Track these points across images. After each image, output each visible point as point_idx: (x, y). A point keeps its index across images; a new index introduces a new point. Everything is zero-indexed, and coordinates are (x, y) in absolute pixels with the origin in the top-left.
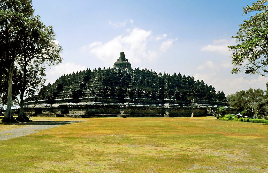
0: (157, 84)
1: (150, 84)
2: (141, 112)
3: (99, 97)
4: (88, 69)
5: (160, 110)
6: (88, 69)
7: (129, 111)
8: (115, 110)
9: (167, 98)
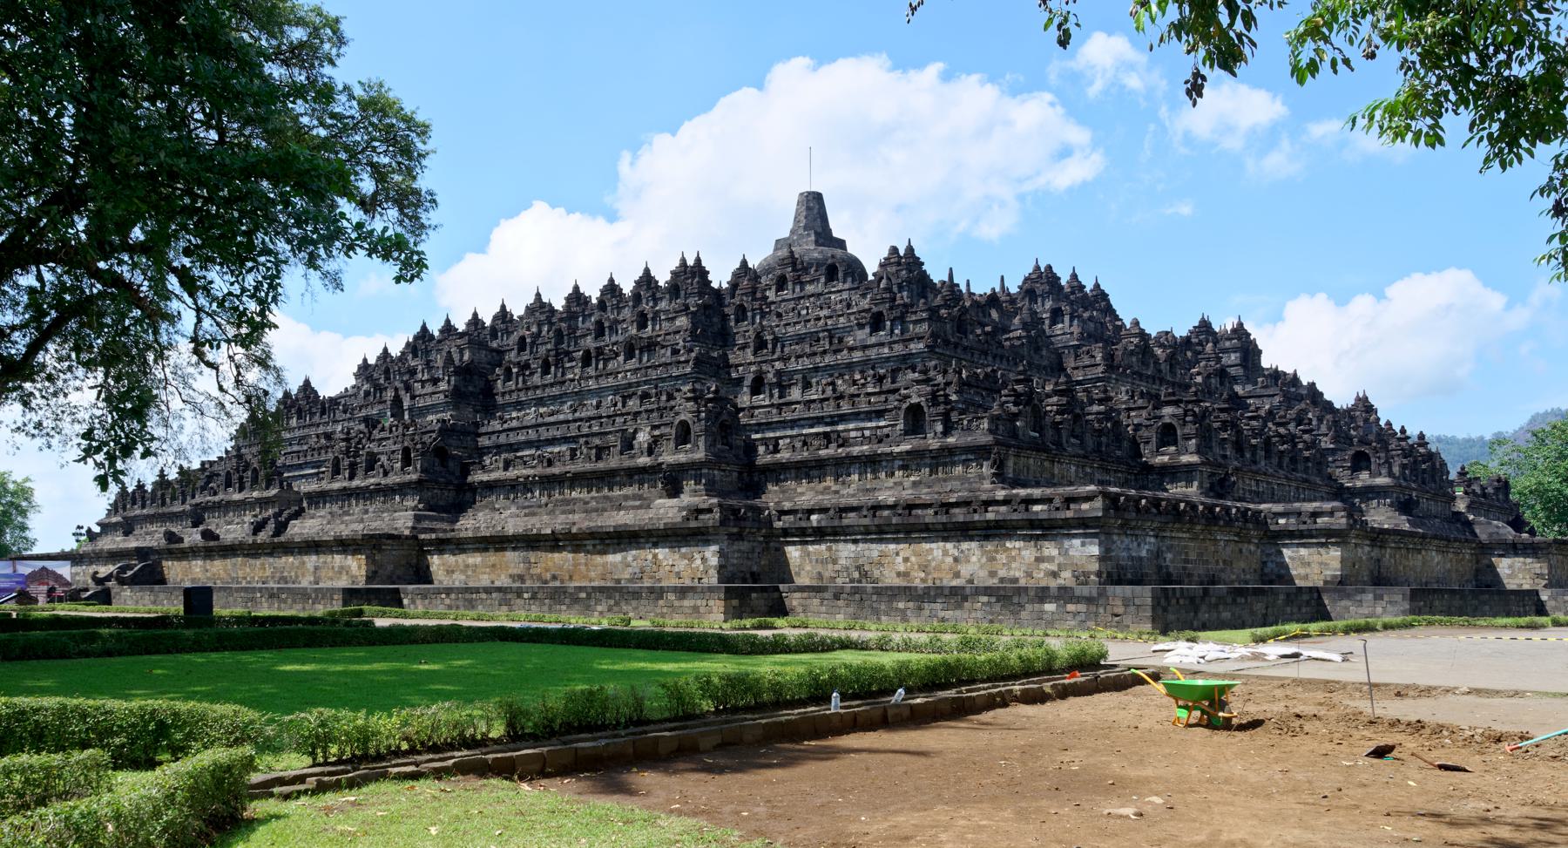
4: (690, 262)
6: (690, 262)
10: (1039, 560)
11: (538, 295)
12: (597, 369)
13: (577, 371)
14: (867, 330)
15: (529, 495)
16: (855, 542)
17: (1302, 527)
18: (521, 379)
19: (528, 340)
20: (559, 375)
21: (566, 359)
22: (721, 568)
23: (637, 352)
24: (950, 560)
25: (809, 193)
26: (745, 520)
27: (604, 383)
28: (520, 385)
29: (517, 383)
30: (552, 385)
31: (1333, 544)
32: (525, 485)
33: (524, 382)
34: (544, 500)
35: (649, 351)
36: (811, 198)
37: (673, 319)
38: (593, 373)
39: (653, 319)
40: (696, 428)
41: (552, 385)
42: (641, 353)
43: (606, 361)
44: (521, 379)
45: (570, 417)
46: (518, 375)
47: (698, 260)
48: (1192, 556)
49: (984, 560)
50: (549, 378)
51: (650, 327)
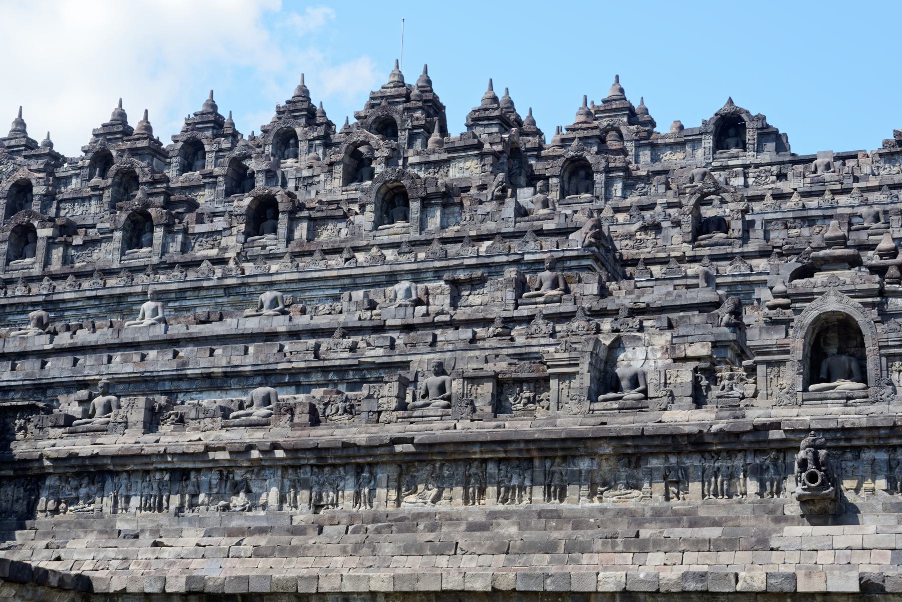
11: (20, 125)
12: (289, 239)
13: (232, 243)
15: (240, 500)
18: (57, 254)
19: (38, 190)
20: (175, 247)
21: (189, 217)
23: (415, 206)
27: (314, 267)
28: (56, 266)
29: (47, 262)
30: (156, 269)
32: (225, 472)
33: (66, 260)
34: (302, 514)
35: (444, 206)
38: (281, 248)
41: (156, 269)
43: (316, 223)
44: (57, 254)
45: (280, 324)
46: (51, 243)
50: (143, 255)
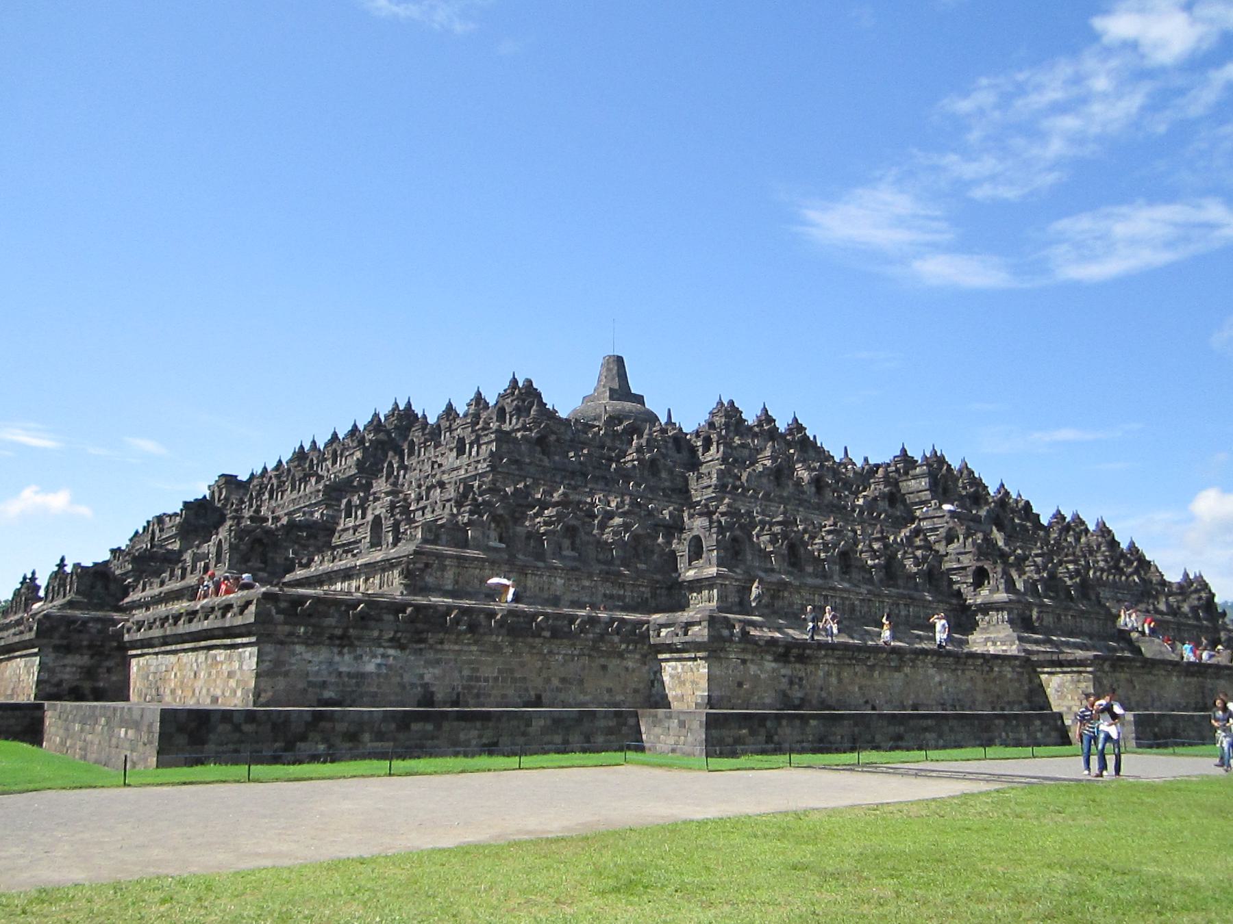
0: (872, 503)
1: (829, 496)
2: (860, 688)
3: (450, 551)
4: (402, 407)
5: (1001, 676)
6: (402, 407)
7: (757, 677)
8: (613, 663)
9: (985, 592)
10: (231, 675)
14: (454, 454)
16: (157, 654)
17: (676, 640)
22: (39, 682)
24: (192, 675)
25: (610, 356)
26: (80, 632)
31: (701, 659)
36: (611, 360)
37: (353, 454)
39: (341, 456)
40: (225, 546)
42: (300, 485)
47: (409, 404)
48: (488, 672)
49: (206, 675)
51: (338, 463)
